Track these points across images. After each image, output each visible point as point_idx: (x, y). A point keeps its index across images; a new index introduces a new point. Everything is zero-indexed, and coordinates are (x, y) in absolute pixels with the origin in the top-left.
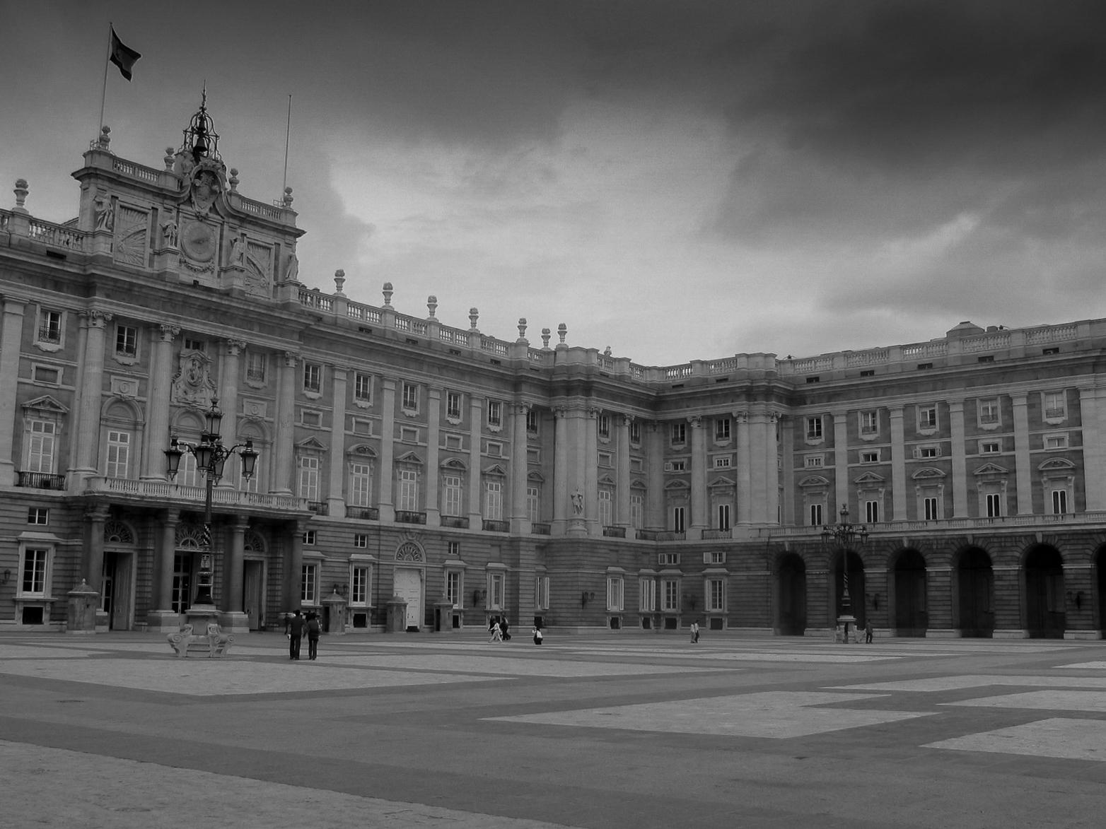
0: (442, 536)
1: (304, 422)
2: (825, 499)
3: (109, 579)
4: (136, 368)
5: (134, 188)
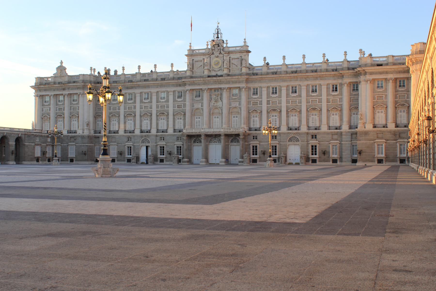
1: (253, 105)
5: (197, 55)
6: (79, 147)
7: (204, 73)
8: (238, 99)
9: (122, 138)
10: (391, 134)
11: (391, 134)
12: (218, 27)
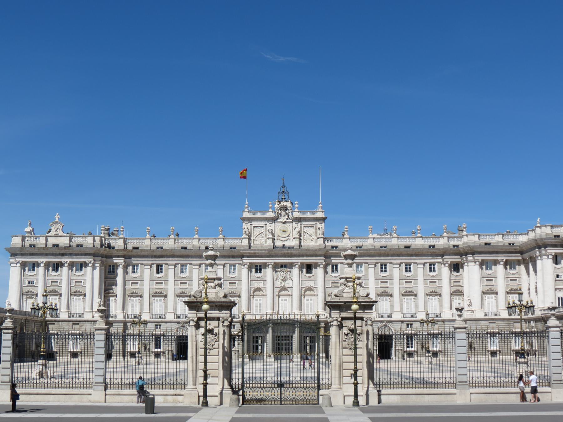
4: (262, 277)
7: (266, 242)
8: (313, 277)
10: (505, 323)
11: (505, 323)
12: (284, 184)
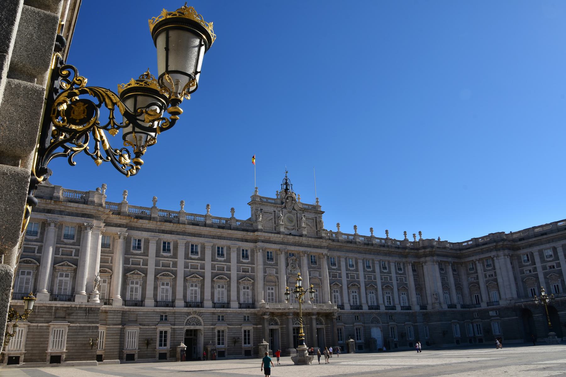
0: (386, 314)
2: (536, 285)
3: (272, 338)
6: (78, 331)
9: (150, 315)
